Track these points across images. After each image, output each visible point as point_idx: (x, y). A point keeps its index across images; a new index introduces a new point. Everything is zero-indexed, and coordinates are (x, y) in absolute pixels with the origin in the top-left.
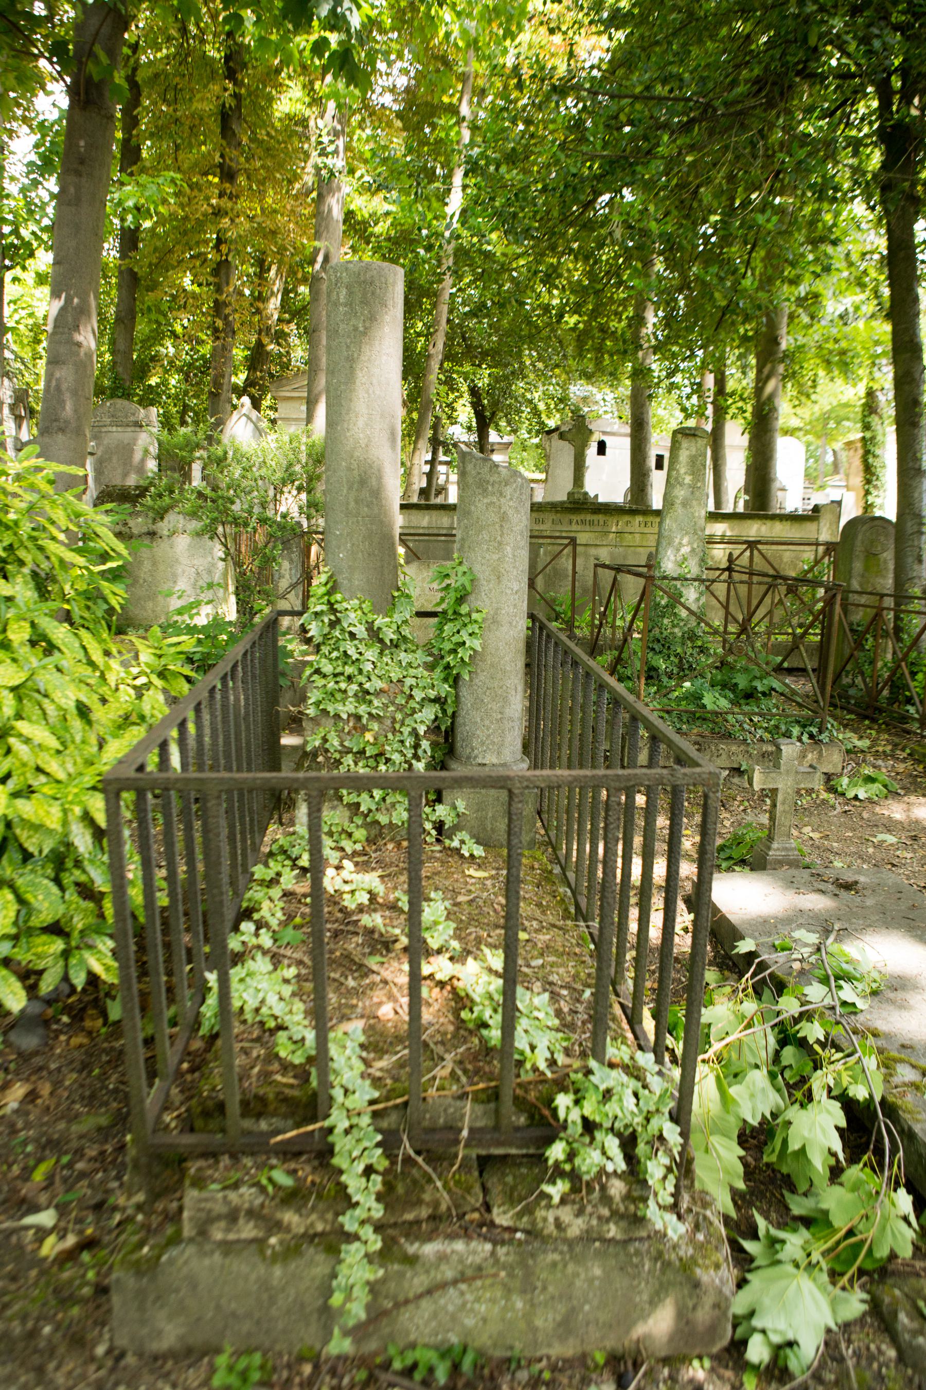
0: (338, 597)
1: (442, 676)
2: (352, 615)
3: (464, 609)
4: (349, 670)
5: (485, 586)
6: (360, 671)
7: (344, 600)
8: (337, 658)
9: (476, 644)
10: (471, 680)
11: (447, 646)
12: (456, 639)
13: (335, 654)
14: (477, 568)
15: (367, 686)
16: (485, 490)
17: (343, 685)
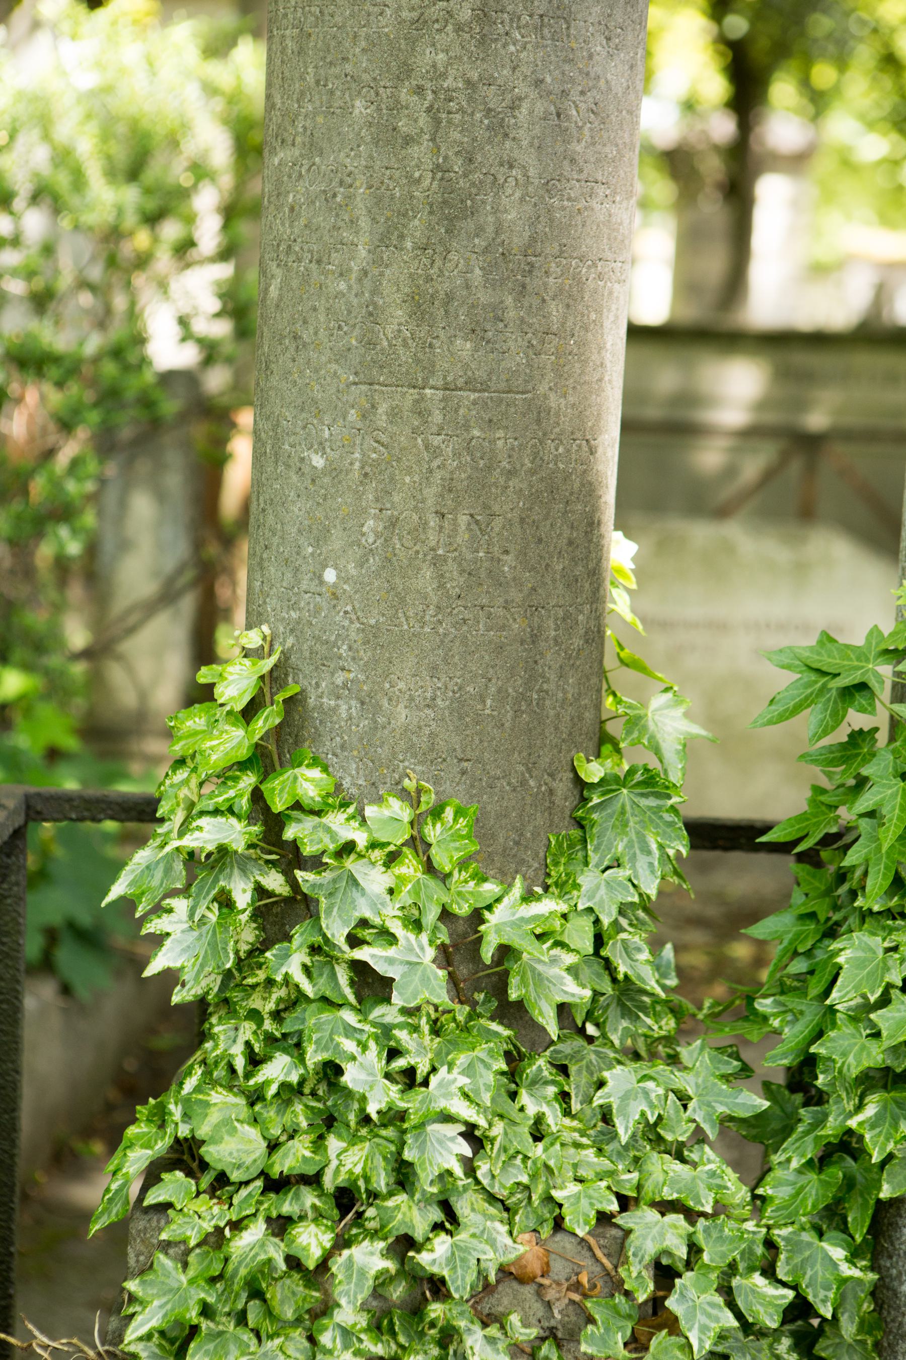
0: (309, 782)
1: (816, 1191)
2: (374, 879)
4: (349, 1159)
6: (404, 1176)
7: (340, 798)
8: (289, 1093)
13: (278, 1070)
15: (435, 1256)
17: (312, 1240)
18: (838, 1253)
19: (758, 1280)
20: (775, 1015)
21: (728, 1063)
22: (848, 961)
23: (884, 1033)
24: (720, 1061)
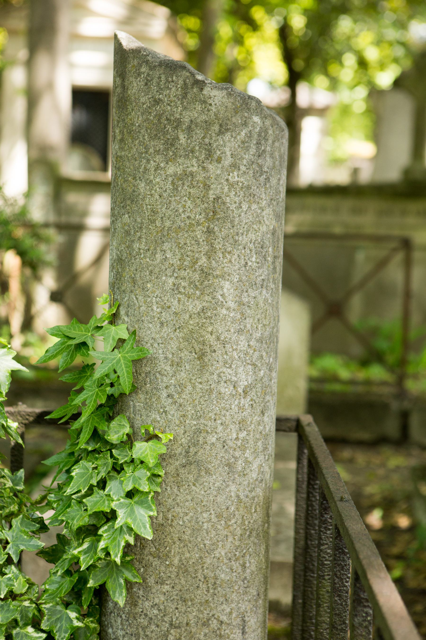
3: (117, 431)
5: (167, 377)
9: (139, 520)
10: (132, 600)
11: (80, 519)
12: (95, 503)
14: (150, 331)
16: (171, 143)
18: (73, 615)
19: (30, 630)
20: (55, 502)
21: (35, 525)
22: (76, 474)
23: (89, 508)
24: (31, 525)
